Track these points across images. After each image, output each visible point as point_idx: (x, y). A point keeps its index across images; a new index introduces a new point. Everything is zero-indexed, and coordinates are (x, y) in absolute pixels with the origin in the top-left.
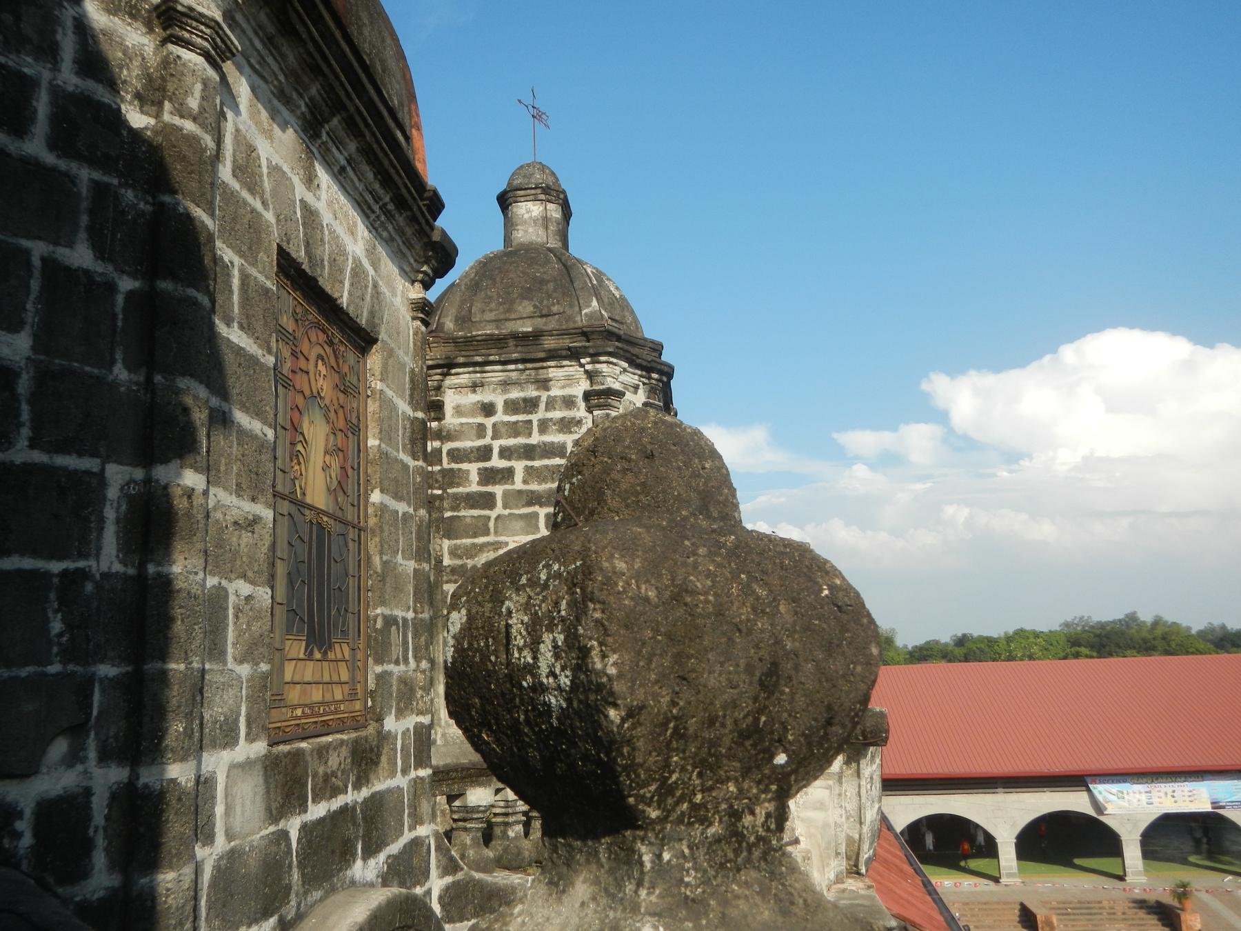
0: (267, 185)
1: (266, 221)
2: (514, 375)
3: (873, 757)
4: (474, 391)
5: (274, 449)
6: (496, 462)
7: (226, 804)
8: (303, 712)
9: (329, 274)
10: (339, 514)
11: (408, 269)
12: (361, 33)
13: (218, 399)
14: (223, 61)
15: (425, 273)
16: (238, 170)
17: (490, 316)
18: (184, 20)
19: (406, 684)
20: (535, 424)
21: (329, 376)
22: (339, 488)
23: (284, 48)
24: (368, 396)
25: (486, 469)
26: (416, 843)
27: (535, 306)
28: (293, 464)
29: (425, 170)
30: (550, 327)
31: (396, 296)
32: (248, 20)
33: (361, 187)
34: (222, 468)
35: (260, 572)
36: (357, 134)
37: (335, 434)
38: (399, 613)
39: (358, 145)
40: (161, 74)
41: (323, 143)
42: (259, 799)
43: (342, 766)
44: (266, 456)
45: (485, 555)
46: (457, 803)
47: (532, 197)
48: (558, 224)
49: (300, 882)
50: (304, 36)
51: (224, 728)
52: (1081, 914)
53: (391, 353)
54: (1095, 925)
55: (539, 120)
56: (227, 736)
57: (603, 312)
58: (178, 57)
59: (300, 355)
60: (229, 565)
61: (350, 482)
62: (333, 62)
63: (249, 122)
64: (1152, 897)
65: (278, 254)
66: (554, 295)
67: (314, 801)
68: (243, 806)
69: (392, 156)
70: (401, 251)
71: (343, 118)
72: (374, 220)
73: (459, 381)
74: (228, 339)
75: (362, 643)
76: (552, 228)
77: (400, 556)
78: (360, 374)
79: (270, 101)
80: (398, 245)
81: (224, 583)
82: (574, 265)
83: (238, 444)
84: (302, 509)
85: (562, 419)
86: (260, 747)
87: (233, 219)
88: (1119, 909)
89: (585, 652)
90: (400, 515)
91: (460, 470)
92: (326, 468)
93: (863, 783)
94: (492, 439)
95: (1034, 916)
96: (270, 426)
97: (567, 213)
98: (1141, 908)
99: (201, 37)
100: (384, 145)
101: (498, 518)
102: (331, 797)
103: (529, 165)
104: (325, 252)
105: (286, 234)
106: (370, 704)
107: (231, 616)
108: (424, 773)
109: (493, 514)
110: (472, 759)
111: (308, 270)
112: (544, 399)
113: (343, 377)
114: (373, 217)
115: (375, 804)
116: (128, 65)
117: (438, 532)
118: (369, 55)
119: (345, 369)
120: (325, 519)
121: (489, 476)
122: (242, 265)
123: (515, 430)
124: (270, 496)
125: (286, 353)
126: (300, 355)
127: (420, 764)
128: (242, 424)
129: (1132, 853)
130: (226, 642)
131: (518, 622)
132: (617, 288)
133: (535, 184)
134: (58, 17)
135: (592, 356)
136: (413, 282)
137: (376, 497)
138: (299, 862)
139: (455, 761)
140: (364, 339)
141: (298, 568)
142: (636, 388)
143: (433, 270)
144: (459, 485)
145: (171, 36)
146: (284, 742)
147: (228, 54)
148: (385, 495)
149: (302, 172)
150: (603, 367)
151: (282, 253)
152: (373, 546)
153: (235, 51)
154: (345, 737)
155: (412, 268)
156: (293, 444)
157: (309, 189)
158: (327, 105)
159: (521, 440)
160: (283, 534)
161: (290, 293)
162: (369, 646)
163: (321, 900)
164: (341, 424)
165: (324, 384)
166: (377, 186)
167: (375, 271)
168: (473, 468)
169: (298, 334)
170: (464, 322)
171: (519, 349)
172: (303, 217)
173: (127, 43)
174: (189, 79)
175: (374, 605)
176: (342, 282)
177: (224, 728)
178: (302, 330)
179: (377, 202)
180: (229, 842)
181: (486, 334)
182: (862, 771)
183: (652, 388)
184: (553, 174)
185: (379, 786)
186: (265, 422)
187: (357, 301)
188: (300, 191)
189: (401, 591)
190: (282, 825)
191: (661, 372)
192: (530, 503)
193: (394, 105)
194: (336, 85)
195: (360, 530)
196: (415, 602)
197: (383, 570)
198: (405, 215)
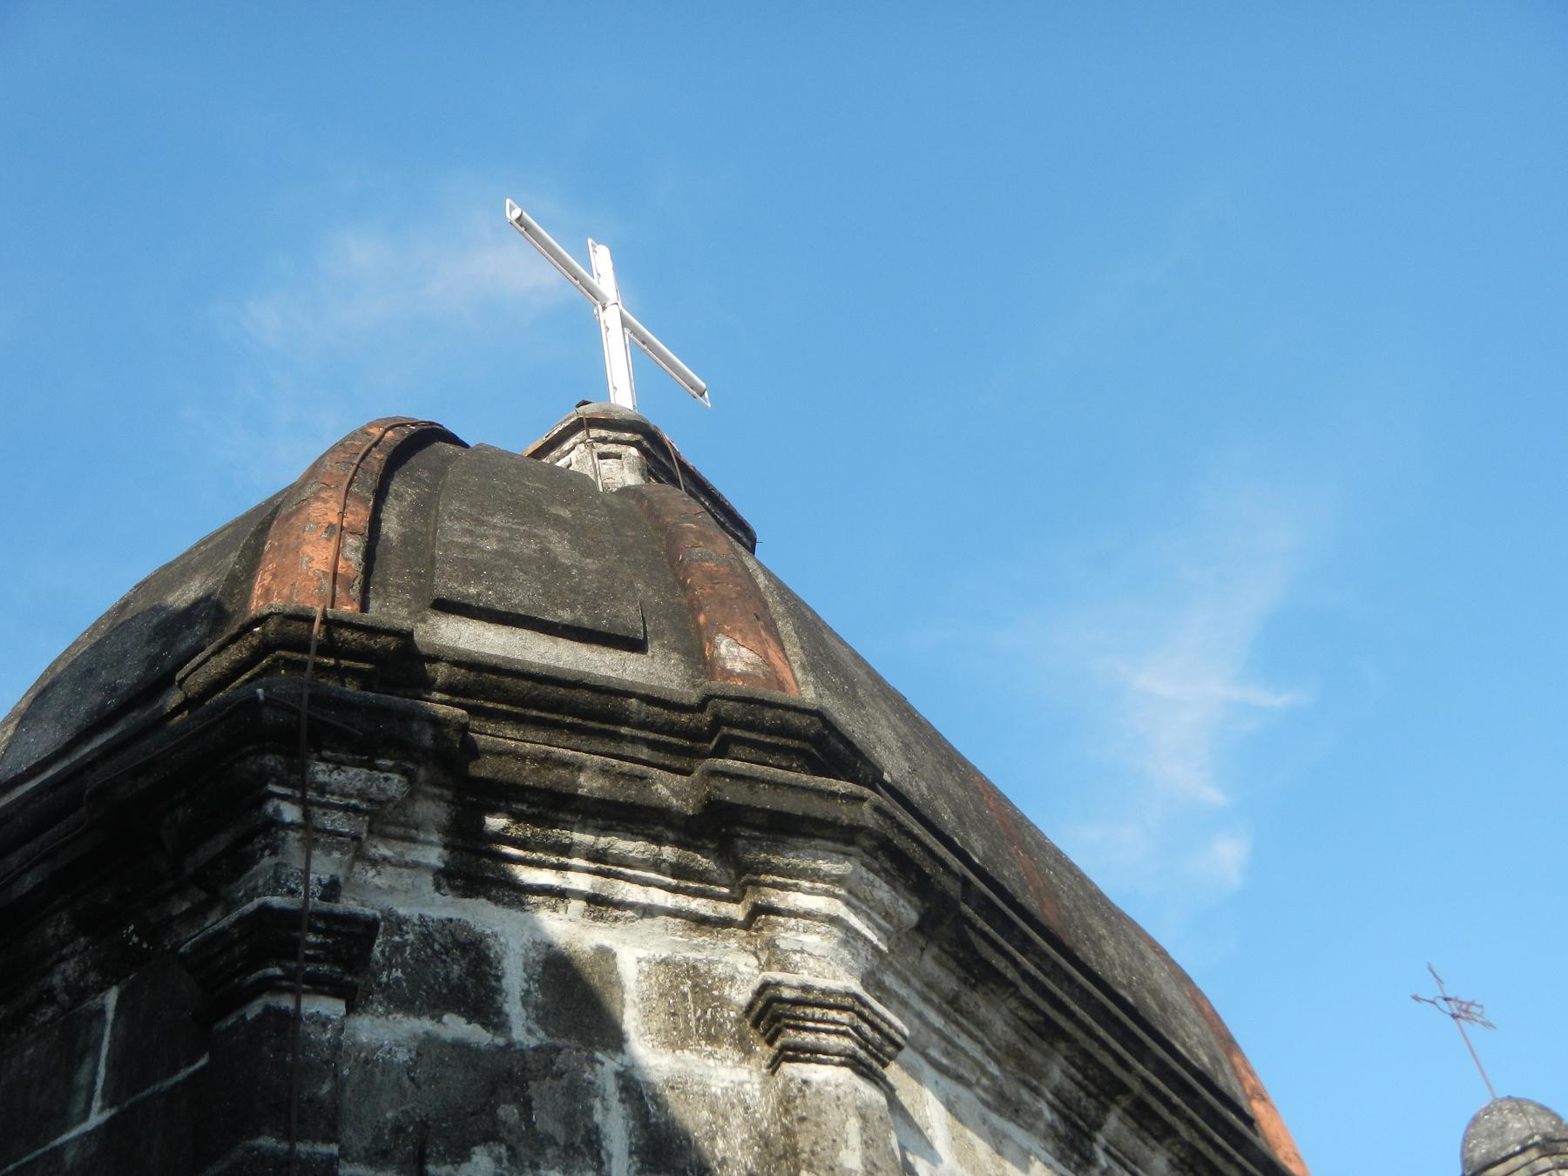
12: (1101, 954)
14: (885, 1065)
18: (799, 1011)
23: (983, 1010)
32: (907, 982)
36: (1164, 1133)
39: (1170, 1156)
40: (783, 1125)
50: (1011, 974)
55: (1468, 1019)
58: (805, 1082)
62: (1074, 1007)
69: (1240, 1158)
71: (1125, 1110)
79: (985, 1121)
99: (836, 1032)
100: (1219, 1139)
103: (1488, 1111)
116: (722, 1128)
118: (1129, 987)
133: (1520, 1142)
134: (591, 1083)
145: (784, 1048)
147: (890, 1049)
153: (899, 1039)
158: (1089, 1094)
173: (713, 1089)
174: (833, 1117)
184: (1544, 1110)
193: (1203, 1064)
194: (1093, 1047)
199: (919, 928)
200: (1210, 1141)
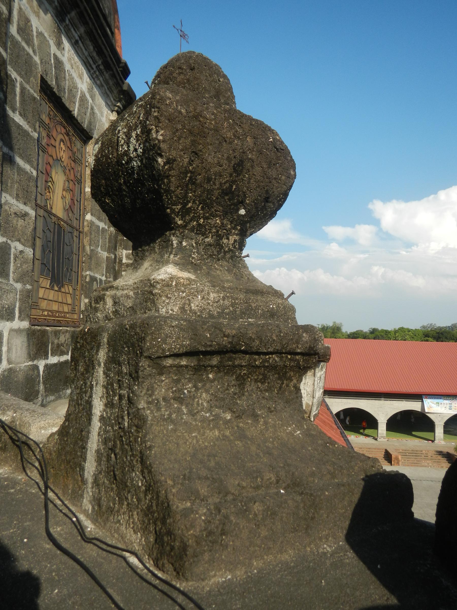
0: (36, 42)
1: (35, 61)
3: (322, 368)
5: (37, 181)
7: (8, 347)
8: (48, 314)
9: (68, 97)
10: (70, 222)
11: (110, 104)
13: (7, 149)
15: (118, 106)
16: (20, 30)
21: (66, 150)
22: (70, 209)
24: (87, 166)
28: (46, 192)
31: (103, 117)
33: (86, 54)
34: (9, 185)
36: (85, 23)
37: (68, 181)
38: (98, 276)
41: (67, 25)
42: (24, 348)
43: (67, 342)
44: (32, 184)
49: (44, 391)
51: (8, 311)
52: (413, 456)
54: (418, 461)
55: (184, 38)
56: (9, 315)
59: (51, 137)
60: (12, 233)
61: (75, 207)
63: (27, 5)
64: (445, 450)
65: (41, 81)
67: (52, 355)
68: (16, 350)
69: (103, 39)
70: (107, 94)
72: (93, 73)
74: (13, 119)
75: (79, 287)
77: (99, 249)
80: (105, 89)
81: (9, 241)
83: (18, 174)
84: (50, 215)
86: (25, 324)
87: (17, 56)
88: (430, 455)
90: (101, 228)
92: (63, 197)
93: (316, 379)
95: (391, 455)
96: (35, 169)
98: (440, 455)
100: (99, 31)
102: (60, 355)
105: (45, 71)
106: (82, 317)
107: (12, 259)
111: (57, 92)
113: (74, 154)
114: (92, 71)
117: (121, 246)
119: (75, 149)
120: (62, 223)
122: (22, 82)
124: (34, 204)
125: (44, 134)
126: (51, 137)
128: (20, 164)
129: (439, 431)
130: (10, 270)
136: (112, 111)
137: (88, 217)
138: (44, 382)
141: (47, 244)
143: (122, 105)
146: (38, 325)
148: (93, 217)
149: (55, 39)
151: (43, 81)
152: (86, 241)
154: (68, 329)
155: (112, 103)
156: (46, 182)
160: (40, 222)
161: (47, 104)
162: (82, 289)
163: (54, 401)
164: (72, 177)
165: (64, 155)
166: (95, 54)
167: (93, 101)
169: (51, 126)
175: (86, 270)
176: (75, 103)
177: (8, 311)
179: (95, 64)
180: (9, 365)
186: (32, 166)
187: (82, 114)
188: (53, 49)
189: (100, 266)
190: (35, 362)
195: (80, 232)
196: (106, 272)
197: (91, 254)
198: (109, 73)
200: (97, 31)
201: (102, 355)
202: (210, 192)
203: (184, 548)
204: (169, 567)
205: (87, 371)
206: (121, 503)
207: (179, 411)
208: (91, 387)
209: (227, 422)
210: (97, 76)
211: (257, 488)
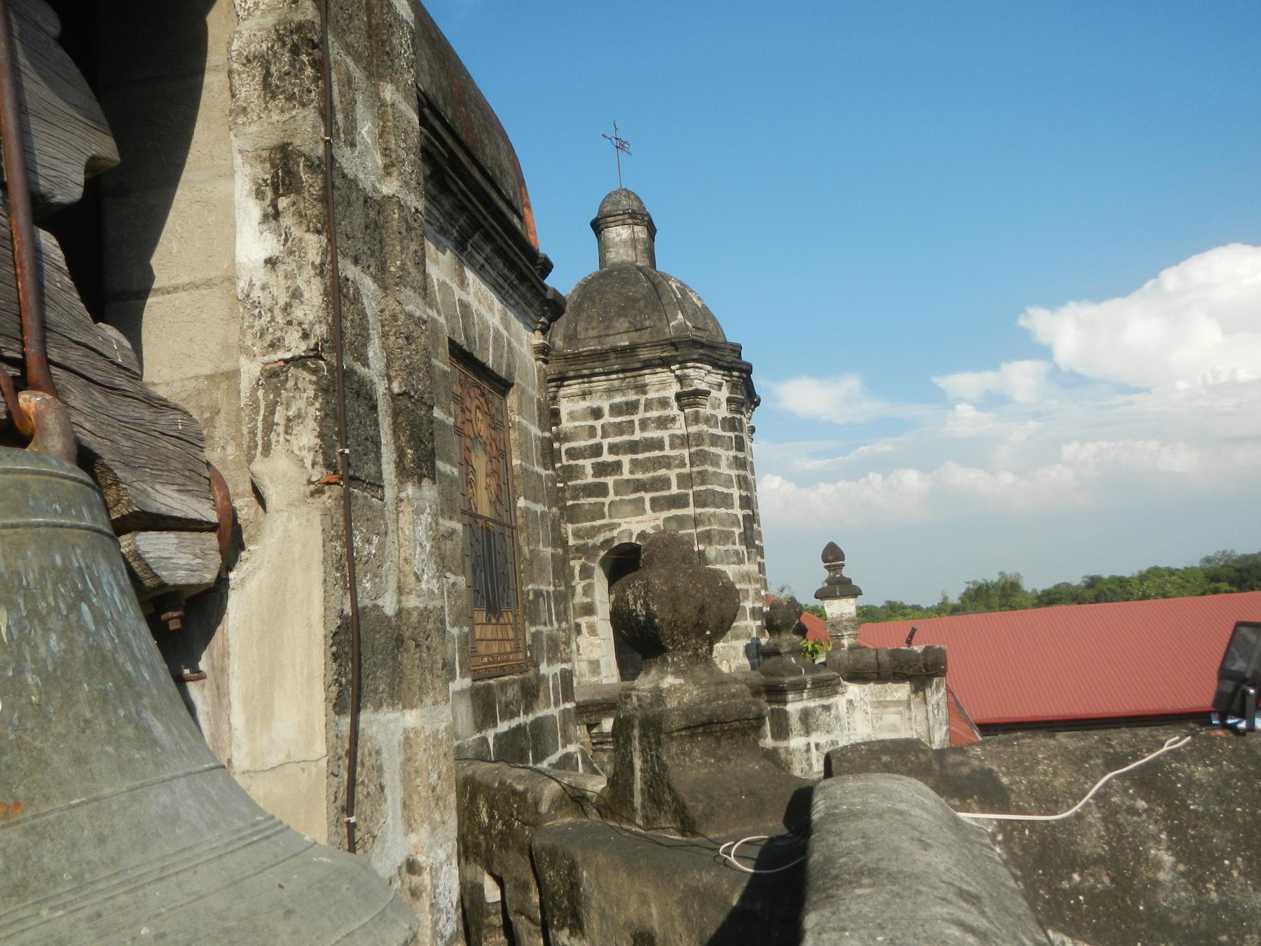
0: (439, 299)
2: (616, 383)
4: (584, 399)
6: (607, 457)
11: (529, 322)
12: (484, 154)
15: (542, 323)
17: (593, 333)
19: (552, 640)
20: (637, 423)
22: (497, 501)
25: (598, 463)
26: (568, 758)
27: (630, 323)
29: (536, 239)
30: (643, 341)
33: (494, 274)
35: (458, 566)
38: (544, 588)
42: (470, 716)
45: (602, 535)
46: (595, 731)
47: (620, 222)
48: (645, 243)
50: (455, 190)
53: (523, 391)
57: (688, 323)
66: (646, 311)
73: (569, 391)
76: (640, 247)
77: (541, 545)
78: (503, 412)
82: (661, 282)
85: (659, 418)
89: (648, 605)
91: (576, 465)
92: (488, 487)
93: (930, 708)
94: (602, 438)
97: (652, 231)
101: (611, 503)
103: (616, 193)
104: (476, 332)
106: (529, 654)
108: (570, 705)
109: (607, 501)
110: (604, 696)
112: (642, 402)
113: (492, 417)
115: (538, 724)
119: (493, 411)
121: (601, 469)
123: (620, 429)
125: (458, 412)
127: (566, 699)
131: (631, 598)
132: (699, 299)
135: (680, 363)
136: (534, 331)
137: (521, 503)
139: (591, 698)
140: (503, 385)
142: (720, 385)
144: (577, 478)
150: (690, 372)
151: (451, 342)
152: (522, 539)
157: (462, 290)
159: (626, 438)
162: (525, 613)
164: (495, 452)
165: (482, 427)
166: (506, 271)
168: (587, 463)
170: (571, 339)
171: (619, 361)
172: (461, 312)
176: (488, 349)
178: (466, 391)
181: (591, 350)
182: (928, 699)
183: (734, 384)
184: (637, 198)
185: (541, 713)
188: (458, 293)
189: (544, 571)
190: (483, 734)
191: (740, 370)
192: (636, 490)
196: (554, 579)
199: (430, 176)
201: (636, 732)
202: (686, 628)
203: (694, 822)
204: (688, 834)
205: (626, 742)
206: (660, 812)
207: (684, 760)
208: (631, 753)
209: (711, 764)
210: (511, 296)
211: (729, 796)
